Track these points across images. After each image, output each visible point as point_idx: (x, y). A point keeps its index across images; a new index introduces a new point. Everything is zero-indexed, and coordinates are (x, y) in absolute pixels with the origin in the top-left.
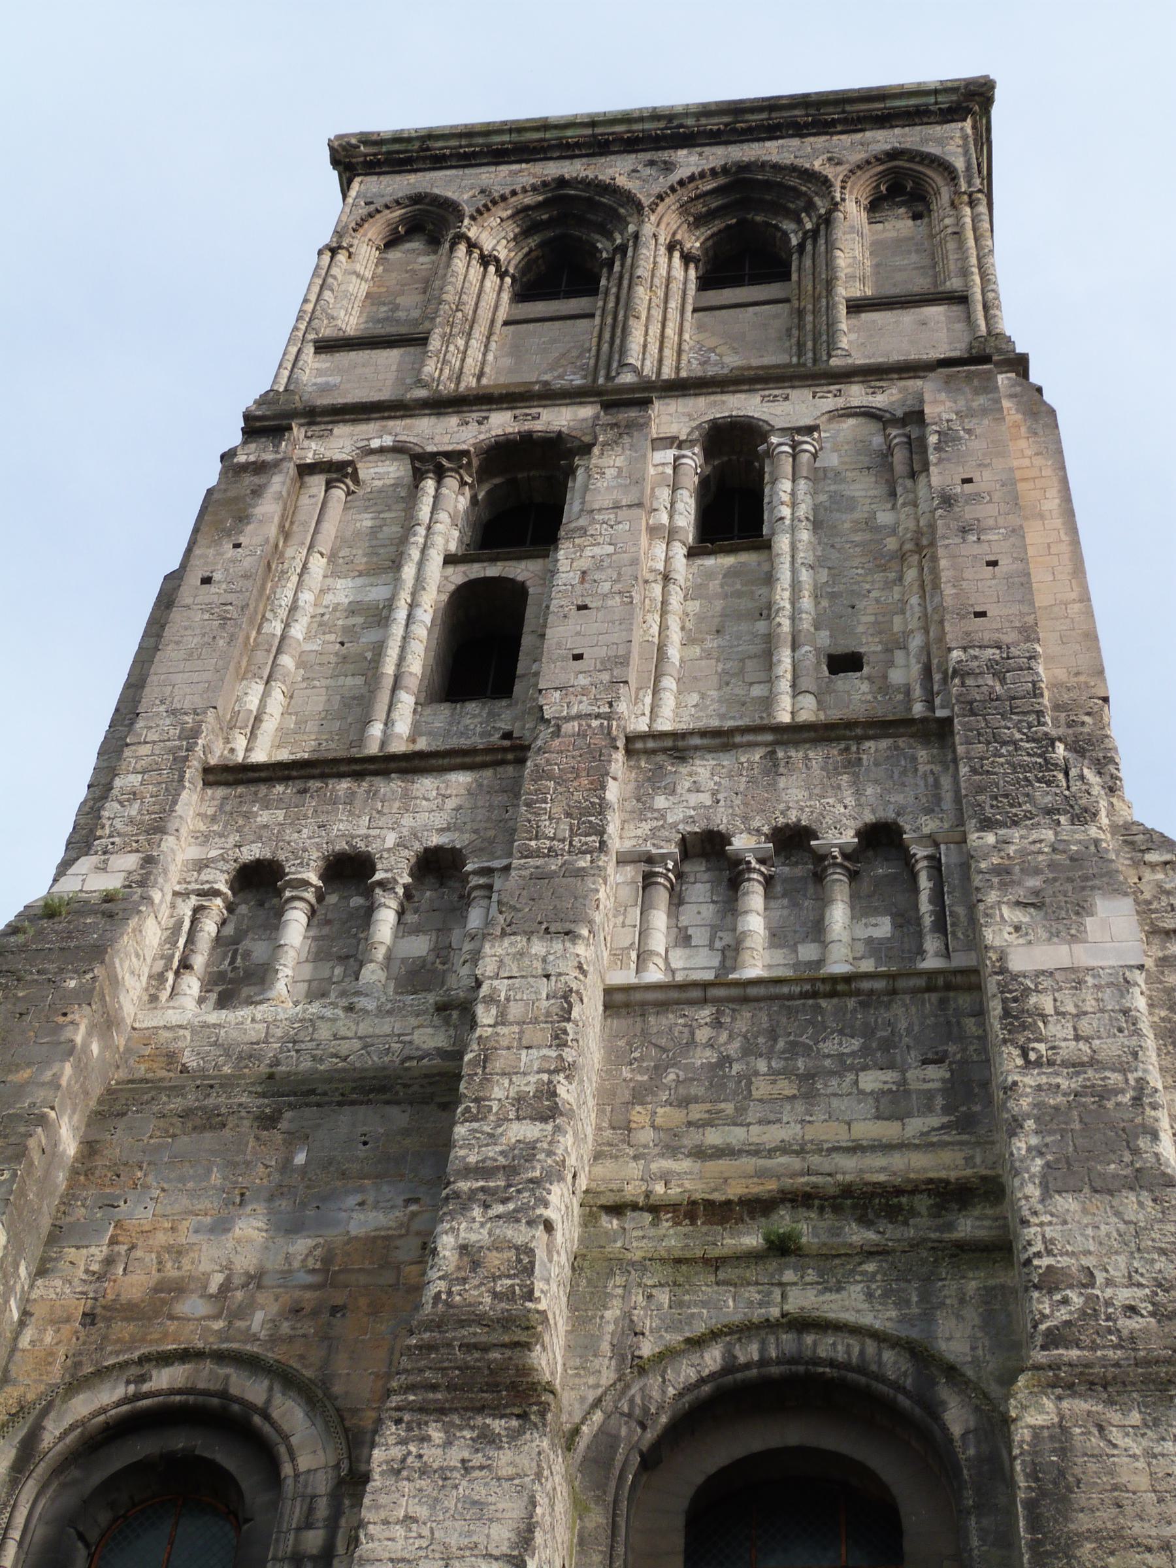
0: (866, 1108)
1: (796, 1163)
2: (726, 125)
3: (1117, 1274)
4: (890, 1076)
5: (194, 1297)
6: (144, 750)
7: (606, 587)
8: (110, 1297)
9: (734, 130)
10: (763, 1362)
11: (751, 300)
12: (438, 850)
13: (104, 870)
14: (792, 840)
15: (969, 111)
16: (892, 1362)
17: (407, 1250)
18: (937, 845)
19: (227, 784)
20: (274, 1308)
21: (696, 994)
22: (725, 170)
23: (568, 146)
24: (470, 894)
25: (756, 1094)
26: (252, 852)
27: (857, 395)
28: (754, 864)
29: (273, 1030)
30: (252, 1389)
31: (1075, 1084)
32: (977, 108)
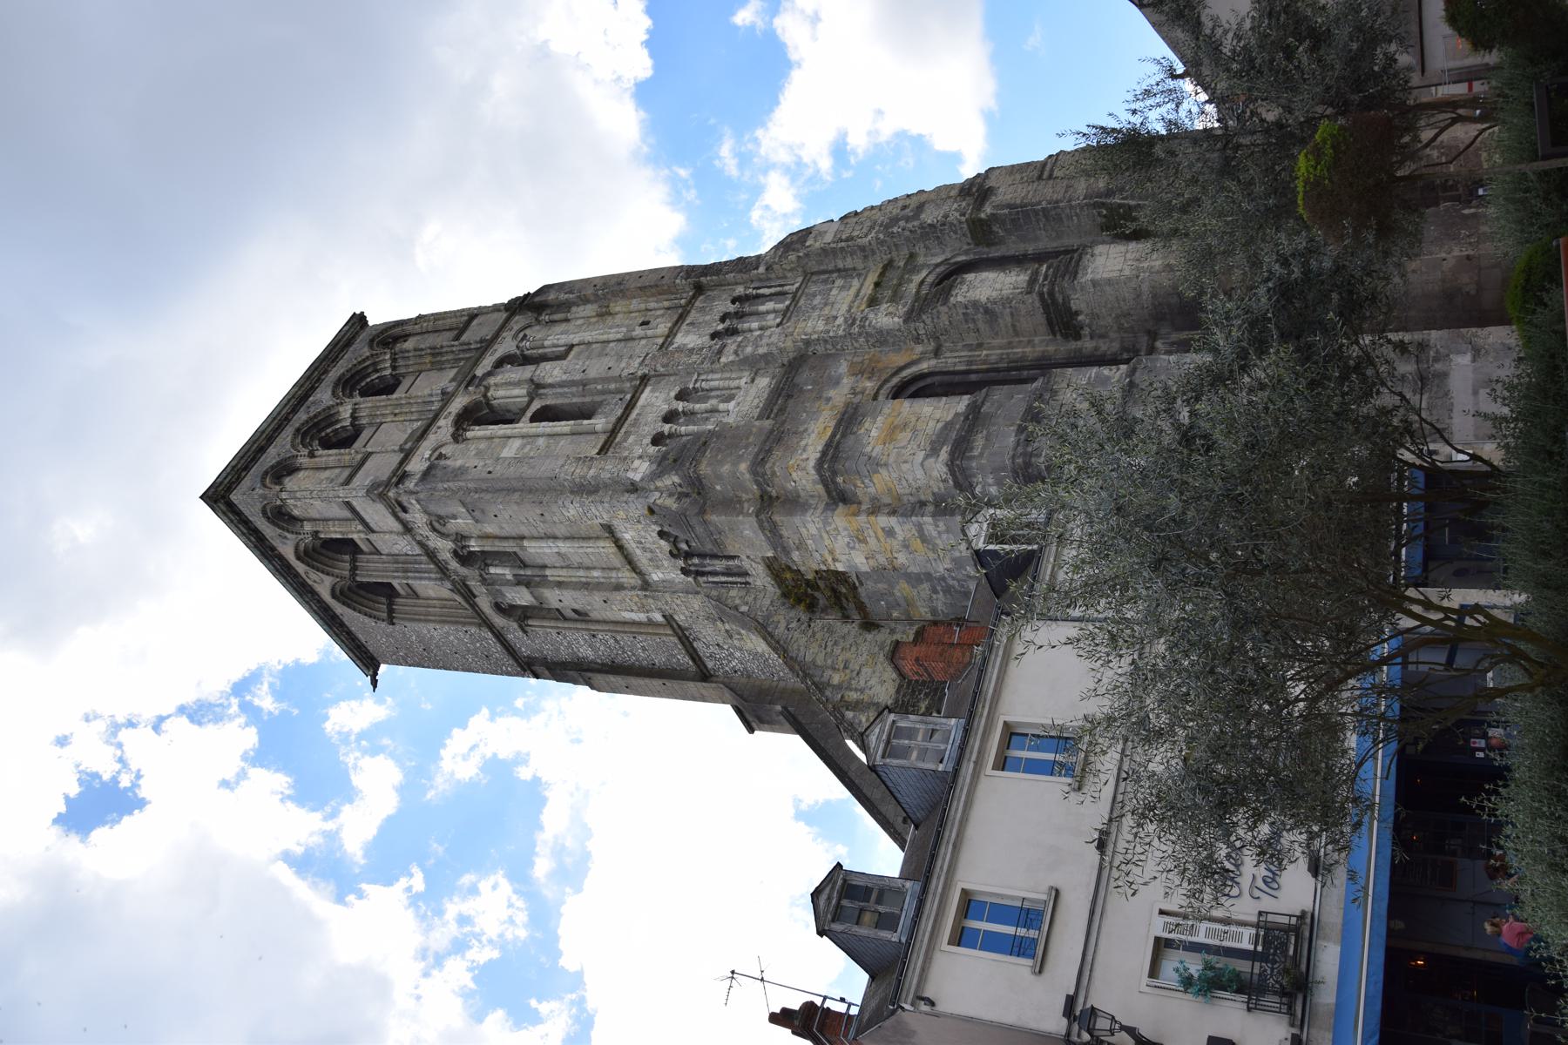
0: (844, 294)
26: (648, 440)
30: (895, 380)
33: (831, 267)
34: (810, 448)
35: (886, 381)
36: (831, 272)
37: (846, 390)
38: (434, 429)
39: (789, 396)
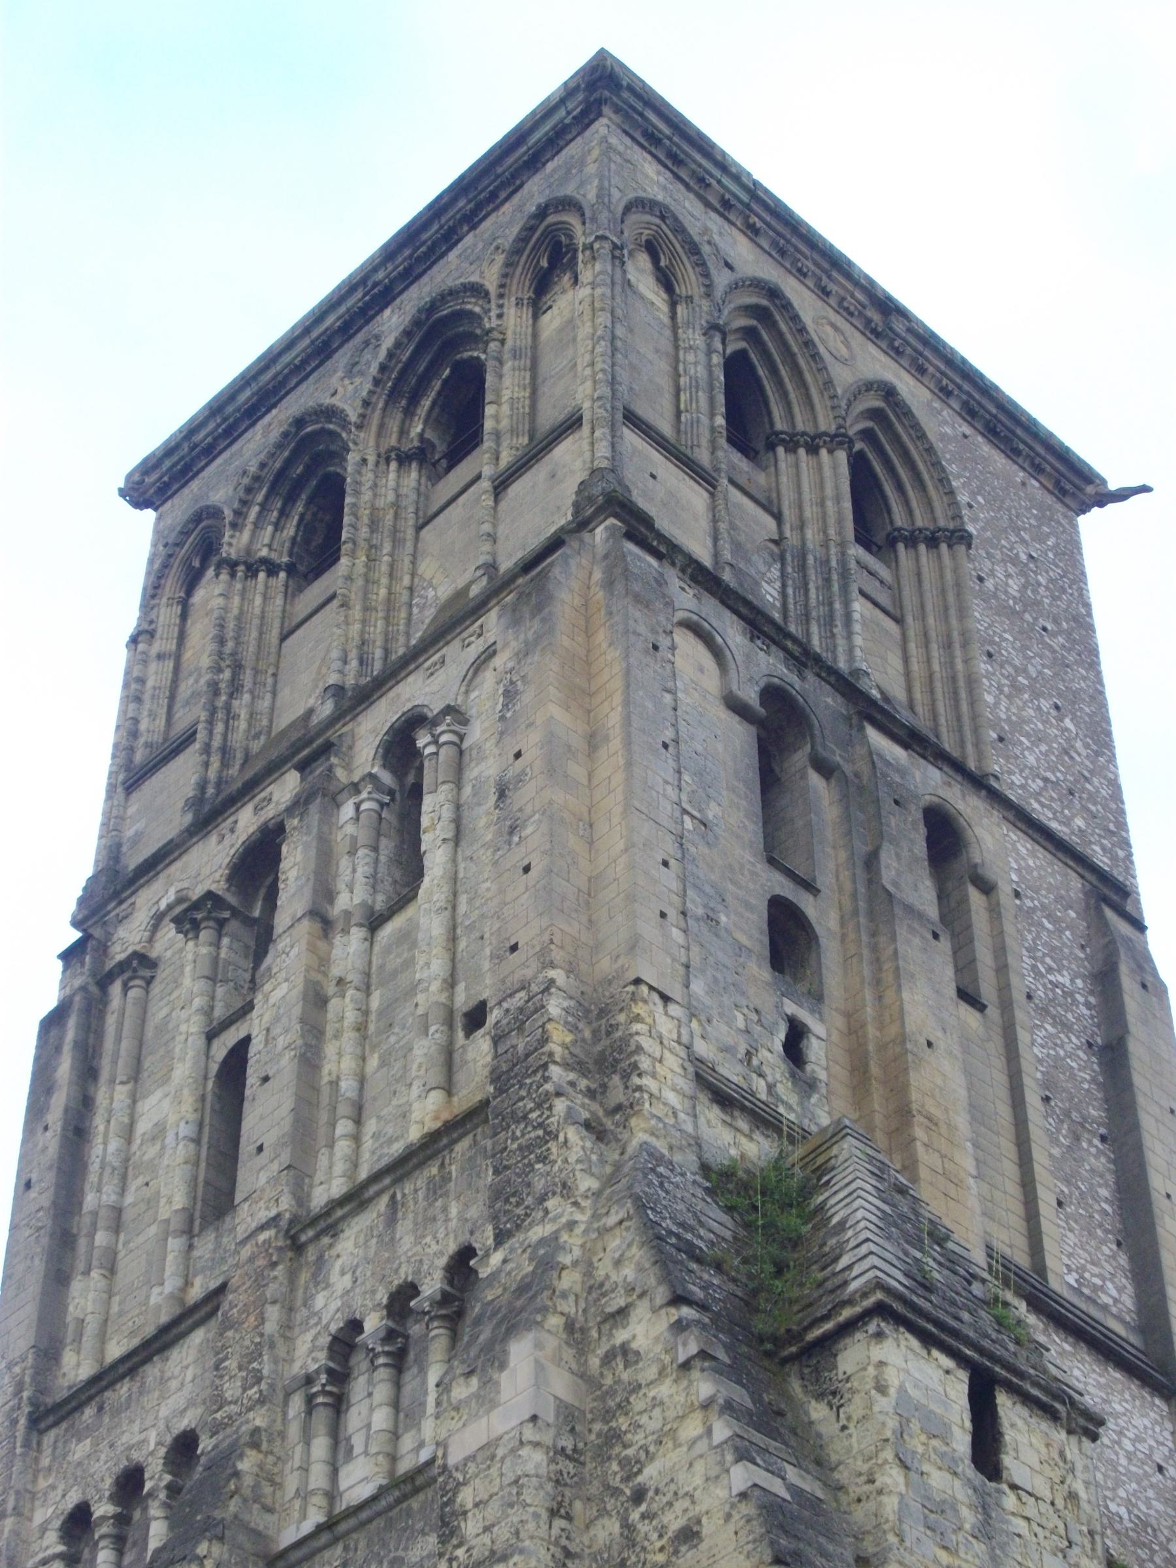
2: (411, 256)
9: (418, 259)
11: (456, 490)
15: (600, 102)
19: (56, 1424)
21: (325, 1538)
22: (417, 323)
23: (297, 369)
28: (379, 1349)
32: (606, 93)
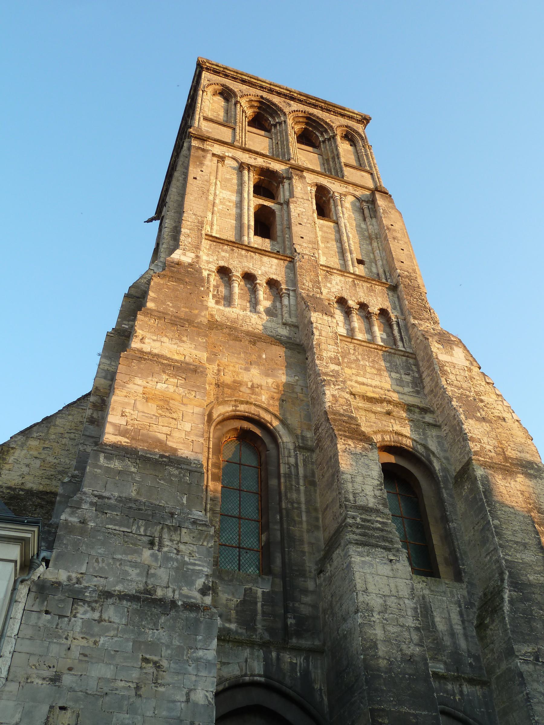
1: (382, 392)
3: (486, 441)
4: (398, 375)
5: (245, 387)
6: (189, 223)
7: (305, 220)
8: (222, 381)
10: (390, 441)
12: (273, 279)
13: (185, 255)
14: (363, 306)
16: (420, 448)
17: (298, 389)
18: (398, 318)
20: (267, 396)
24: (282, 294)
25: (368, 371)
26: (222, 263)
27: (351, 189)
29: (239, 317)
31: (460, 392)
33: (422, 369)
34: (158, 344)
35: (267, 410)
36: (418, 371)
37: (257, 381)
38: (254, 156)
39: (254, 344)
